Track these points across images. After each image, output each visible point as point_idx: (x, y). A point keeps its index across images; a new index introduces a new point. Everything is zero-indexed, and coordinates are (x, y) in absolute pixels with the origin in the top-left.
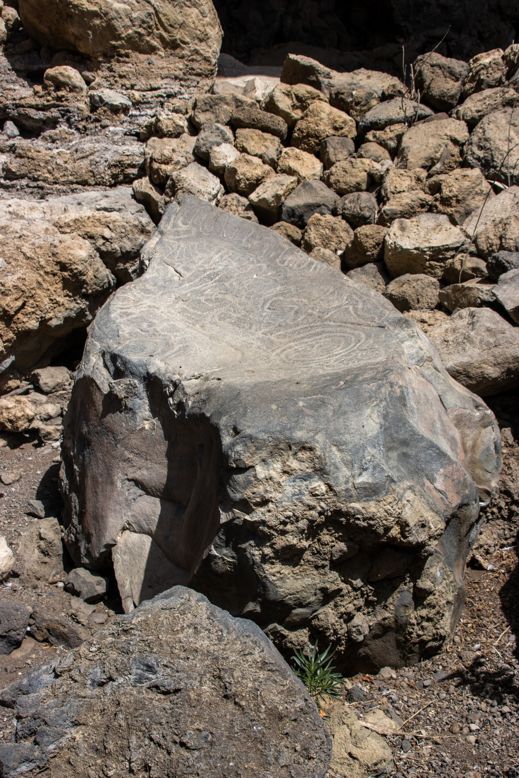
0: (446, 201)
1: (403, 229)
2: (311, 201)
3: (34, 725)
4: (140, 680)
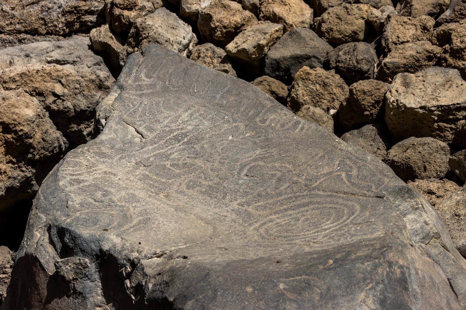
0: (457, 54)
1: (406, 84)
2: (298, 52)
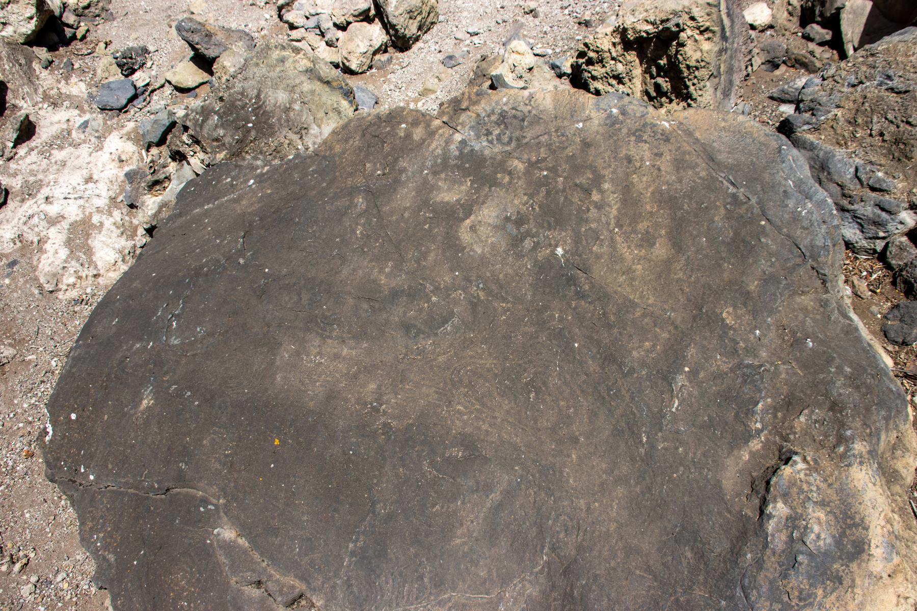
3: (812, 105)
4: (880, 84)
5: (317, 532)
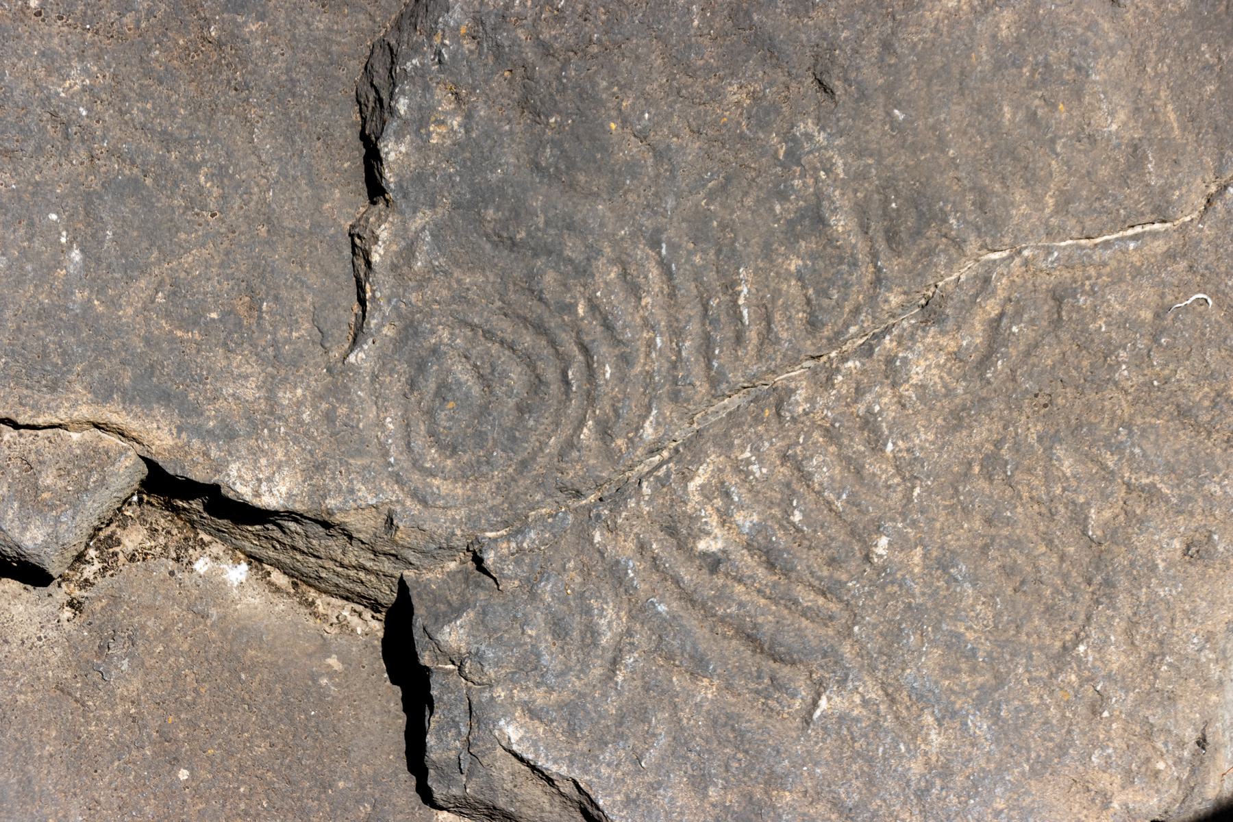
5: (167, 140)
